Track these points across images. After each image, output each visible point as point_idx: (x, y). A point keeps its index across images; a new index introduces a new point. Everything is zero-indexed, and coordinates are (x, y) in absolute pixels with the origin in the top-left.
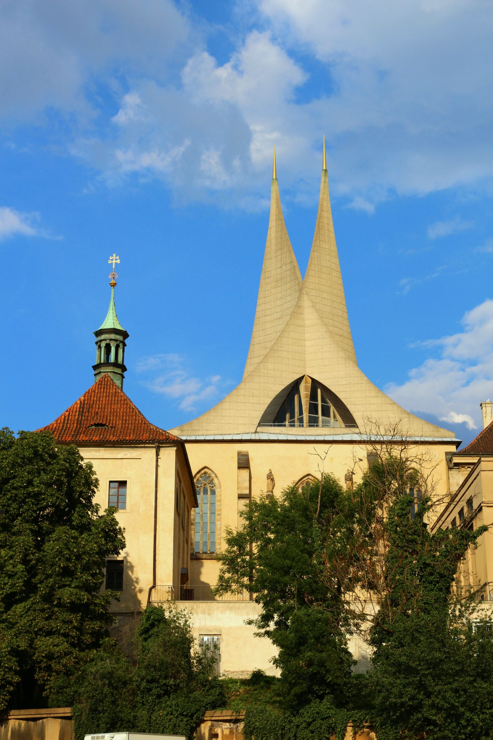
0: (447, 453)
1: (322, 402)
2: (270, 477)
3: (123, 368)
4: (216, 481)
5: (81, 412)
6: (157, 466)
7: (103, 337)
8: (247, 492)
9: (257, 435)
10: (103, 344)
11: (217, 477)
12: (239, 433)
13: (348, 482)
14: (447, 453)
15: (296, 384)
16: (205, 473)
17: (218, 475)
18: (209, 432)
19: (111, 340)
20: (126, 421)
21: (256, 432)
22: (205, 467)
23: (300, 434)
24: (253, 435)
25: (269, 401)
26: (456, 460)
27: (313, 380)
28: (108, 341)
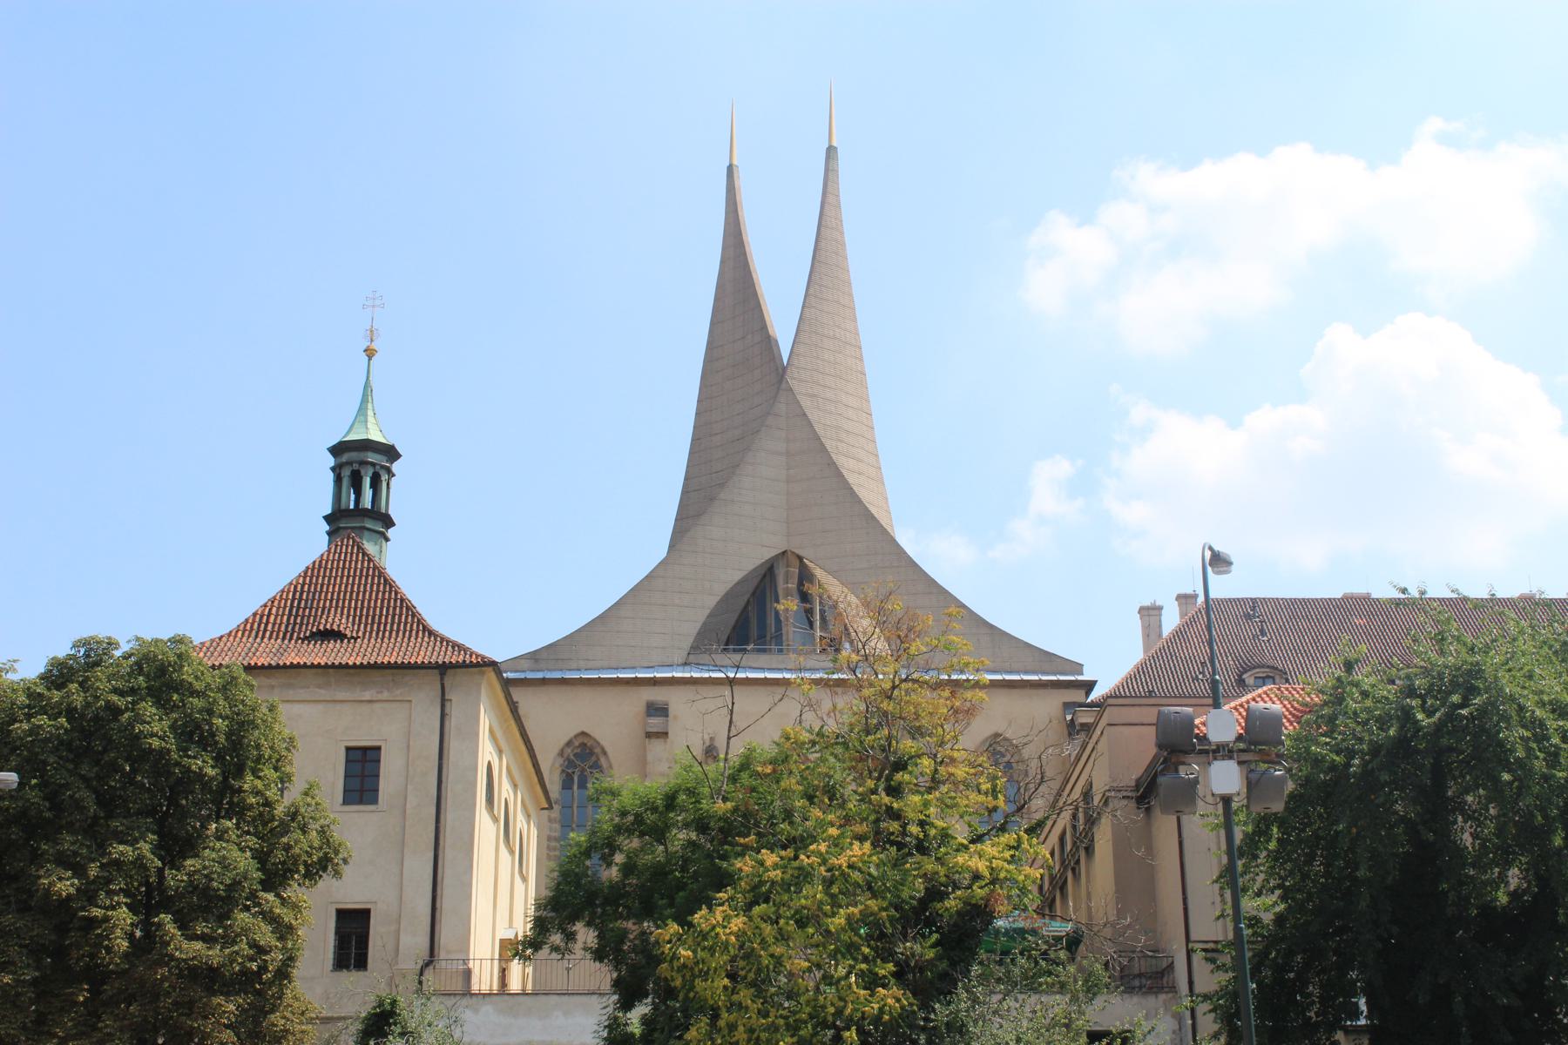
0: (1067, 706)
3: (388, 522)
4: (603, 760)
7: (345, 458)
10: (346, 472)
11: (605, 753)
16: (583, 745)
17: (609, 750)
18: (590, 664)
21: (686, 664)
22: (583, 734)
25: (711, 602)
28: (356, 466)
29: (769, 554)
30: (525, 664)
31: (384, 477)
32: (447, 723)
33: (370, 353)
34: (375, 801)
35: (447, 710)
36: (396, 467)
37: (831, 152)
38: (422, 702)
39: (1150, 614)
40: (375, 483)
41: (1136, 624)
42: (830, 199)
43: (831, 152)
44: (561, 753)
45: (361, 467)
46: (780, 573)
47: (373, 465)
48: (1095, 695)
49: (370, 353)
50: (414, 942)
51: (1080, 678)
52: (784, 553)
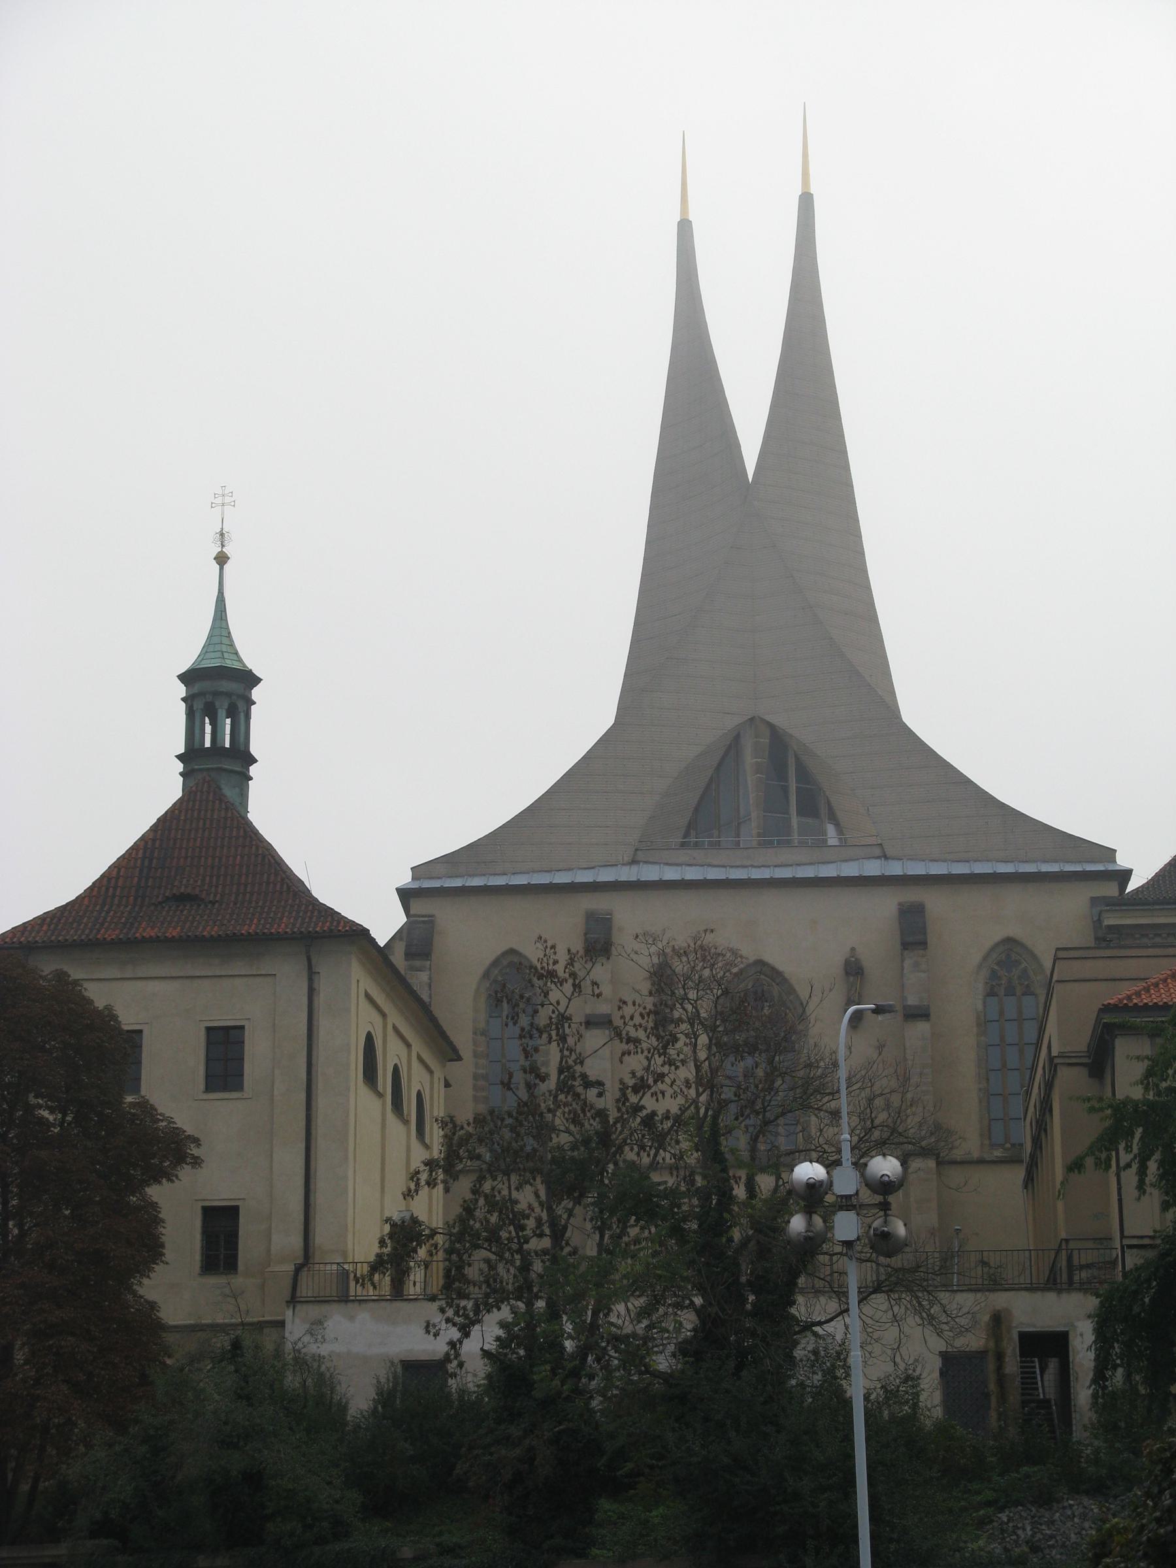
0: (1094, 901)
1: (797, 782)
6: (311, 992)
9: (635, 868)
12: (593, 864)
13: (852, 979)
14: (1094, 901)
19: (216, 694)
20: (246, 886)
21: (634, 862)
22: (512, 951)
23: (738, 863)
24: (626, 869)
26: (1110, 920)
27: (772, 728)
28: (209, 698)
31: (241, 705)
32: (315, 998)
33: (222, 559)
34: (239, 1087)
35: (315, 986)
36: (256, 693)
38: (287, 974)
44: (486, 975)
45: (219, 691)
47: (228, 694)
48: (1132, 886)
50: (288, 1241)
51: (1111, 867)
52: (752, 719)
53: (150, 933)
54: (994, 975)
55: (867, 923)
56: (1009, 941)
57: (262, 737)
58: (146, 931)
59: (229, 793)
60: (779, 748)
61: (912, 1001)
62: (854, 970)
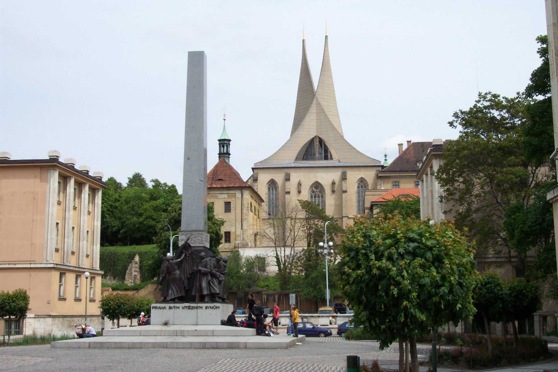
2: (300, 184)
3: (230, 154)
5: (213, 175)
6: (242, 196)
8: (288, 190)
15: (312, 140)
22: (272, 179)
25: (299, 149)
27: (320, 138)
29: (312, 137)
30: (259, 164)
33: (224, 120)
37: (326, 37)
38: (238, 194)
39: (400, 145)
40: (227, 146)
41: (397, 147)
42: (326, 53)
43: (326, 37)
46: (315, 140)
49: (224, 120)
53: (215, 186)
54: (359, 184)
55: (336, 175)
56: (362, 178)
57: (232, 150)
58: (214, 186)
59: (227, 160)
60: (321, 141)
61: (344, 189)
62: (333, 183)
